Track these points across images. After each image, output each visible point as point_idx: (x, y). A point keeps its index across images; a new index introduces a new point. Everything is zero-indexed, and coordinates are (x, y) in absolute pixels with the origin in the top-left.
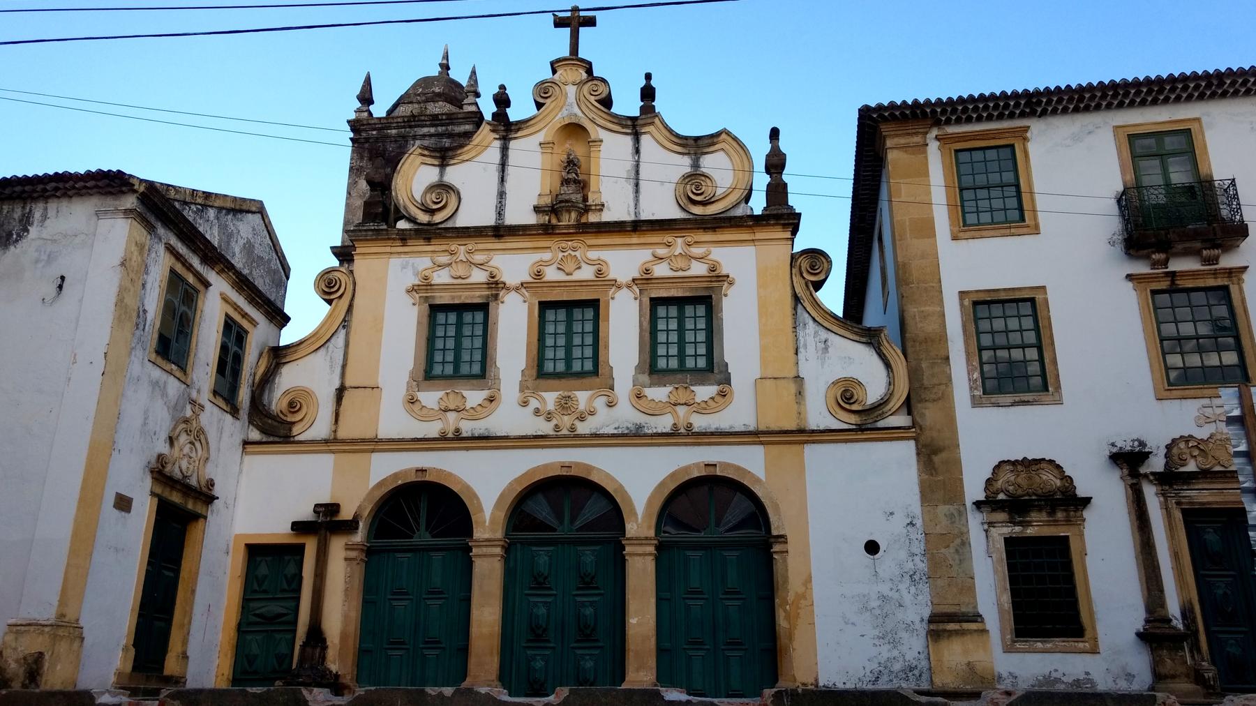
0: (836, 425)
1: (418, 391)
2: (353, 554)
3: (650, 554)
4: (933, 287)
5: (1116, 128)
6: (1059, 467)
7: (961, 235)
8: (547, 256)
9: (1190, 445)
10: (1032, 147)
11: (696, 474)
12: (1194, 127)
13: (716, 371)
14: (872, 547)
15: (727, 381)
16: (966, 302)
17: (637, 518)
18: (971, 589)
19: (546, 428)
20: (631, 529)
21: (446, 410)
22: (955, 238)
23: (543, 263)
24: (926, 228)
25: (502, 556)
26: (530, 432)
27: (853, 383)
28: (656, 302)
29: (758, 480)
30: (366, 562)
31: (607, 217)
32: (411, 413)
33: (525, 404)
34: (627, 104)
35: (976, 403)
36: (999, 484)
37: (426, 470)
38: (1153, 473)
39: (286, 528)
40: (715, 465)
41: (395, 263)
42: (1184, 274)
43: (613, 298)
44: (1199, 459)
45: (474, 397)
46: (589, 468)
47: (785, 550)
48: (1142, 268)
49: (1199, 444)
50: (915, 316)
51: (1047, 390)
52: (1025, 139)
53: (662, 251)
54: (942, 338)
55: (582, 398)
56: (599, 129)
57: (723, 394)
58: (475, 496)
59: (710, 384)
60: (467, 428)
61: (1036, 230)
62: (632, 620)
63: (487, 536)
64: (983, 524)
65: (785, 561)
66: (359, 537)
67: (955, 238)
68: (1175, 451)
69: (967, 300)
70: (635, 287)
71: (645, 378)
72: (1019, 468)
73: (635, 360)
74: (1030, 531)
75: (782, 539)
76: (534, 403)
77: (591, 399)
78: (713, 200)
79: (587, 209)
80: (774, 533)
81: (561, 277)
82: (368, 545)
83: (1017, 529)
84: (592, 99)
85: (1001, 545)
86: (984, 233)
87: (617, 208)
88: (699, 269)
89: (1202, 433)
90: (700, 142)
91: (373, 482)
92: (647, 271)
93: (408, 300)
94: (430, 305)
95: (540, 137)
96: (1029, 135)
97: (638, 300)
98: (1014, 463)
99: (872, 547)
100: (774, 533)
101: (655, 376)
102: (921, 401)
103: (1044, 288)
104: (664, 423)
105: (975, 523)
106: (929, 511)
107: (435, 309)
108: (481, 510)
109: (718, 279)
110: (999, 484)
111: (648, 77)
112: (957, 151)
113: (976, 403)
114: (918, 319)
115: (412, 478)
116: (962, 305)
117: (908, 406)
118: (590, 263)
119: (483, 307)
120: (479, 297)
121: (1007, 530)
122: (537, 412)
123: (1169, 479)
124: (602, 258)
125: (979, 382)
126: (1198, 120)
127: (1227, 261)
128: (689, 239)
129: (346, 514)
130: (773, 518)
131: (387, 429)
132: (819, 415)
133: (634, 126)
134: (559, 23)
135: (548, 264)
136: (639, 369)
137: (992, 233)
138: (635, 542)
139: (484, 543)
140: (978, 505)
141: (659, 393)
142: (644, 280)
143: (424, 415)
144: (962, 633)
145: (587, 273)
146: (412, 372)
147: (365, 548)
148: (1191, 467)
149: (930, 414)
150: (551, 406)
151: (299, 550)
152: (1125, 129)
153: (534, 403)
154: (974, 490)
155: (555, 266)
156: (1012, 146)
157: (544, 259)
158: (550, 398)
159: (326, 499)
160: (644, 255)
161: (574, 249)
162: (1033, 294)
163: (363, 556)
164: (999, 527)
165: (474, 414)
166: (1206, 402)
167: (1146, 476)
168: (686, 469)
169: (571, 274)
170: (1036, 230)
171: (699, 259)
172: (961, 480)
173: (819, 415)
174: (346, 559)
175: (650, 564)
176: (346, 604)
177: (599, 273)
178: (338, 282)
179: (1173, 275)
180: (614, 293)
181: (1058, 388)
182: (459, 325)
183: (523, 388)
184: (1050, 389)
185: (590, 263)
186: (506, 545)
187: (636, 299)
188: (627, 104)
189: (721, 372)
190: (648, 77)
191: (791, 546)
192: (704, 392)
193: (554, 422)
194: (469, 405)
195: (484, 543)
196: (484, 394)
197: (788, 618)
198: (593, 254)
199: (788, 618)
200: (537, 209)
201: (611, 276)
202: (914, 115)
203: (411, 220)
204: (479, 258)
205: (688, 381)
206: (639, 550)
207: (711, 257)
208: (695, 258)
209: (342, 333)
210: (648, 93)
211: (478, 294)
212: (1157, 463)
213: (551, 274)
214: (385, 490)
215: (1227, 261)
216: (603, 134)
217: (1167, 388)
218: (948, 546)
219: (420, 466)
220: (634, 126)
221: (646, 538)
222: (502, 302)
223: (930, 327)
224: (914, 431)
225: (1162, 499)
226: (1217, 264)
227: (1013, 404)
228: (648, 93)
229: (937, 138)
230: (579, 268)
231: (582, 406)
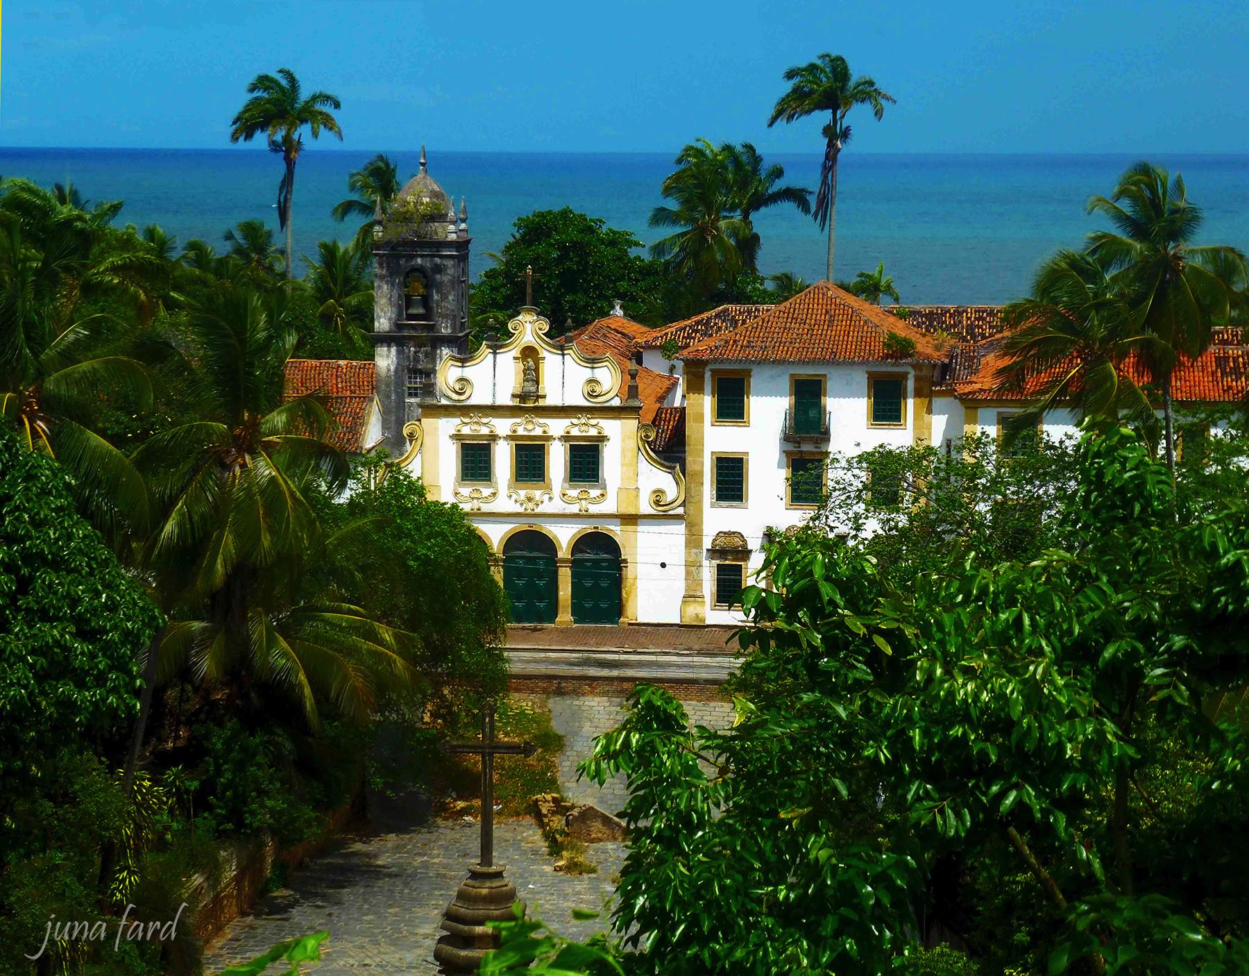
0: (654, 512)
5: (792, 375)
8: (518, 420)
10: (752, 380)
16: (714, 457)
18: (701, 585)
20: (560, 555)
24: (700, 418)
52: (750, 376)
53: (575, 421)
54: (701, 473)
60: (486, 508)
62: (561, 593)
71: (567, 485)
73: (562, 476)
74: (727, 562)
75: (625, 561)
76: (514, 496)
79: (538, 397)
87: (552, 400)
88: (593, 432)
92: (568, 432)
98: (725, 533)
104: (574, 509)
109: (602, 438)
117: (683, 504)
121: (718, 562)
126: (825, 375)
132: (646, 508)
141: (574, 493)
144: (695, 601)
149: (692, 509)
150: (523, 498)
154: (707, 544)
158: (523, 494)
160: (566, 422)
165: (486, 500)
175: (569, 571)
177: (545, 432)
179: (801, 452)
181: (747, 501)
196: (492, 490)
197: (626, 593)
199: (626, 593)
200: (514, 396)
203: (448, 398)
209: (419, 455)
223: (697, 468)
231: (537, 498)
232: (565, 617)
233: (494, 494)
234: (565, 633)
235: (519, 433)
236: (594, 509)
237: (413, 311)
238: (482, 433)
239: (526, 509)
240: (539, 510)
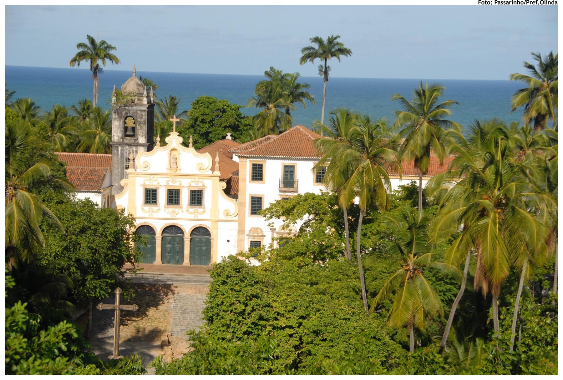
8: (169, 179)
14: (228, 241)
19: (169, 216)
22: (250, 182)
23: (168, 181)
24: (245, 180)
35: (249, 216)
46: (178, 224)
53: (193, 180)
54: (245, 203)
57: (204, 211)
58: (156, 228)
67: (250, 182)
71: (189, 207)
76: (167, 211)
77: (178, 211)
88: (200, 185)
99: (228, 241)
104: (192, 217)
105: (246, 237)
113: (249, 216)
118: (179, 181)
132: (222, 217)
135: (170, 181)
140: (247, 235)
143: (146, 212)
153: (167, 211)
154: (247, 232)
160: (189, 180)
177: (180, 184)
183: (165, 207)
185: (179, 181)
198: (179, 180)
204: (155, 179)
213: (171, 184)
231: (177, 212)
232: (187, 261)
234: (187, 269)
235: (169, 185)
236: (200, 217)
237: (128, 133)
240: (177, 217)
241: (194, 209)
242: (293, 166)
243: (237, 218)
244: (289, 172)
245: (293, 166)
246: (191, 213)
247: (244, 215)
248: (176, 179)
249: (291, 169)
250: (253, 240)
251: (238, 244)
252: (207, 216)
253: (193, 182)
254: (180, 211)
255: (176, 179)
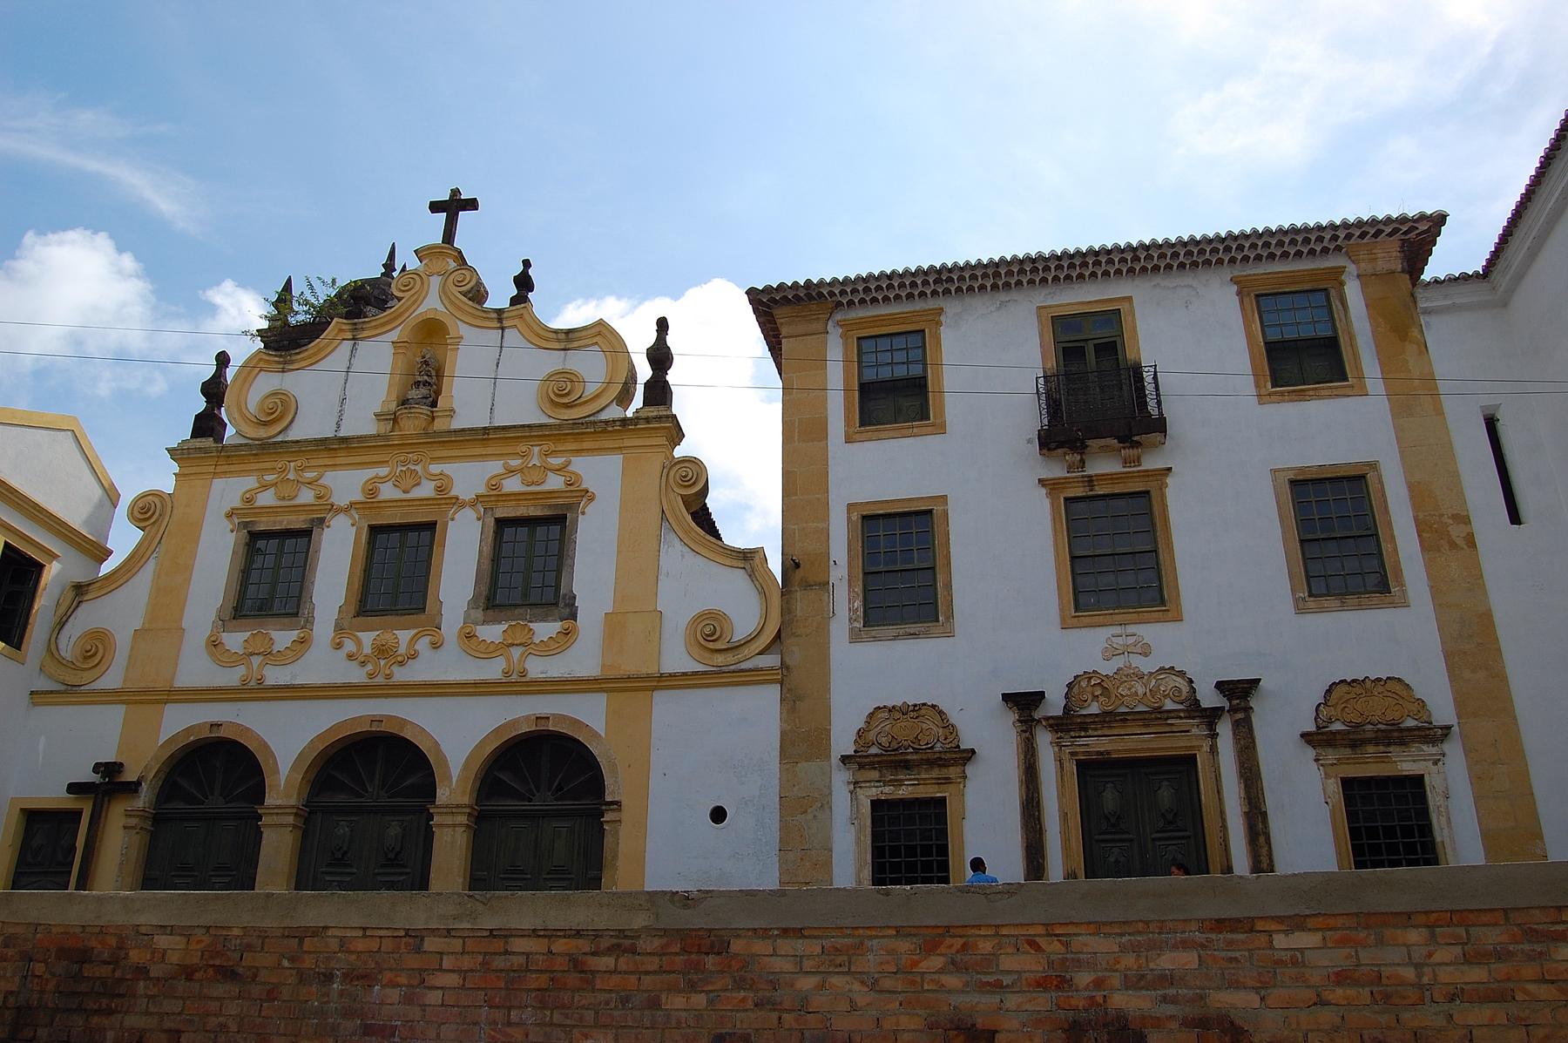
1: (224, 631)
2: (133, 821)
3: (460, 825)
4: (819, 499)
6: (941, 713)
7: (857, 437)
8: (383, 471)
9: (1093, 683)
11: (525, 729)
12: (1124, 307)
13: (561, 605)
14: (718, 815)
15: (573, 616)
16: (855, 517)
17: (451, 782)
19: (357, 675)
20: (443, 795)
21: (252, 654)
25: (295, 826)
26: (340, 680)
27: (718, 616)
28: (501, 523)
29: (596, 735)
30: (152, 832)
31: (457, 424)
32: (211, 655)
33: (339, 646)
34: (500, 295)
35: (855, 637)
36: (872, 736)
37: (221, 725)
38: (1047, 719)
39: (63, 793)
40: (549, 718)
41: (218, 484)
42: (1101, 477)
43: (453, 519)
44: (1102, 699)
45: (283, 638)
46: (403, 723)
47: (618, 819)
48: (1057, 471)
49: (1103, 681)
50: (794, 533)
51: (938, 621)
52: (939, 324)
53: (515, 463)
55: (404, 636)
56: (459, 323)
59: (555, 620)
60: (276, 676)
61: (941, 429)
63: (279, 802)
64: (849, 783)
65: (617, 832)
66: (143, 800)
67: (849, 440)
68: (1075, 690)
69: (856, 514)
70: (479, 505)
72: (897, 715)
73: (469, 592)
76: (350, 646)
77: (414, 639)
78: (582, 400)
80: (608, 798)
81: (398, 495)
82: (154, 812)
83: (887, 789)
84: (455, 290)
85: (866, 809)
86: (883, 435)
88: (555, 483)
89: (1107, 668)
90: (571, 335)
91: (163, 738)
93: (227, 525)
94: (248, 532)
95: (394, 336)
96: (943, 318)
97: (481, 522)
98: (892, 709)
99: (718, 815)
100: (608, 798)
101: (490, 612)
102: (794, 635)
103: (944, 497)
104: (493, 670)
105: (841, 779)
106: (787, 769)
107: (255, 536)
108: (276, 771)
110: (872, 736)
111: (527, 264)
112: (859, 339)
113: (855, 637)
114: (797, 538)
115: (206, 734)
116: (849, 519)
118: (431, 477)
119: (306, 533)
120: (303, 521)
121: (874, 792)
122: (350, 657)
123: (1065, 725)
124: (446, 472)
125: (860, 613)
126: (1129, 299)
127: (1151, 462)
128: (545, 447)
129: (130, 776)
130: (608, 781)
131: (184, 680)
132: (677, 658)
133: (500, 320)
134: (435, 207)
135: (384, 480)
136: (473, 603)
137: (892, 434)
138: (445, 810)
139: (276, 811)
141: (492, 632)
142: (489, 499)
145: (426, 490)
146: (220, 610)
147: (151, 816)
148: (1094, 709)
150: (367, 650)
151: (77, 814)
152: (1049, 310)
154: (843, 741)
155: (390, 483)
156: (923, 331)
157: (381, 474)
158: (368, 638)
159: (110, 757)
160: (495, 467)
161: (417, 463)
162: (930, 505)
163: (148, 825)
164: (866, 787)
166: (1117, 630)
167: (1039, 721)
168: (513, 723)
169: (408, 492)
170: (941, 429)
171: (558, 470)
172: (829, 731)
173: (677, 658)
174: (125, 827)
176: (120, 879)
177: (439, 489)
178: (153, 504)
179: (1090, 481)
180: (455, 513)
181: (950, 616)
182: (280, 552)
183: (339, 628)
184: (941, 618)
185: (431, 477)
186: (306, 815)
187: (479, 519)
188: (500, 295)
189: (566, 605)
190: (527, 264)
191: (625, 815)
192: (545, 630)
193: (370, 667)
194: (276, 648)
195: (276, 811)
196: (294, 635)
198: (435, 468)
201: (453, 493)
202: (810, 297)
205: (528, 617)
206: (449, 820)
207: (570, 468)
208: (551, 470)
210: (524, 283)
211: (302, 518)
212: (1055, 704)
213: (388, 492)
214: (174, 748)
215: (1151, 462)
216: (464, 330)
217: (1074, 614)
218: (805, 812)
219: (215, 719)
220: (500, 320)
221: (458, 806)
222: (328, 527)
224: (783, 676)
225: (1056, 749)
226: (1139, 465)
227: (896, 638)
228: (524, 283)
229: (839, 324)
230: (418, 484)
231: (402, 650)
233: (303, 642)
235: (382, 497)
236: (538, 668)
238: (300, 501)
239: (371, 676)
240: (401, 675)
241: (504, 626)
242: (1112, 317)
243: (771, 660)
244: (1090, 350)
245: (1112, 317)
246: (488, 652)
247: (823, 631)
248: (418, 468)
249: (1103, 333)
250: (887, 792)
251: (785, 828)
252: (583, 659)
253: (511, 472)
254: (423, 645)
255: (418, 468)
